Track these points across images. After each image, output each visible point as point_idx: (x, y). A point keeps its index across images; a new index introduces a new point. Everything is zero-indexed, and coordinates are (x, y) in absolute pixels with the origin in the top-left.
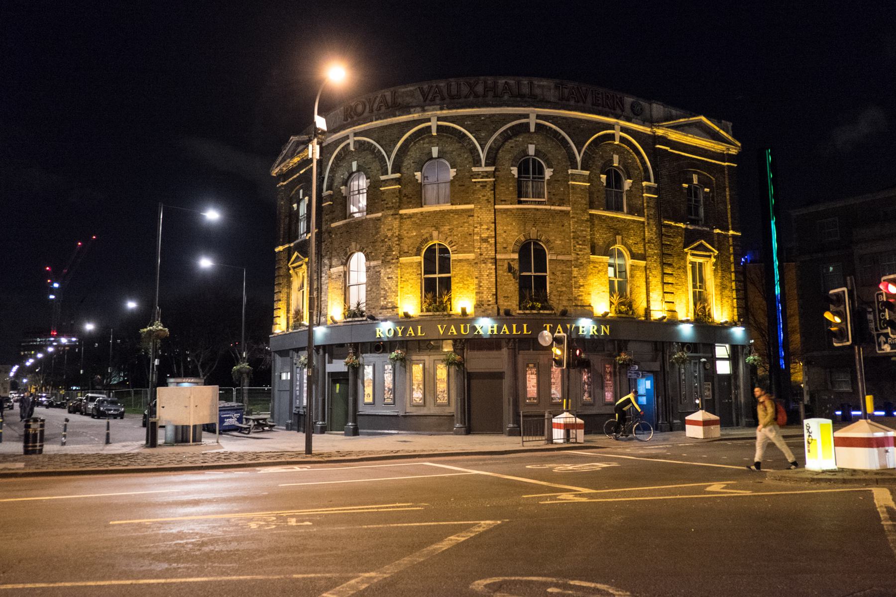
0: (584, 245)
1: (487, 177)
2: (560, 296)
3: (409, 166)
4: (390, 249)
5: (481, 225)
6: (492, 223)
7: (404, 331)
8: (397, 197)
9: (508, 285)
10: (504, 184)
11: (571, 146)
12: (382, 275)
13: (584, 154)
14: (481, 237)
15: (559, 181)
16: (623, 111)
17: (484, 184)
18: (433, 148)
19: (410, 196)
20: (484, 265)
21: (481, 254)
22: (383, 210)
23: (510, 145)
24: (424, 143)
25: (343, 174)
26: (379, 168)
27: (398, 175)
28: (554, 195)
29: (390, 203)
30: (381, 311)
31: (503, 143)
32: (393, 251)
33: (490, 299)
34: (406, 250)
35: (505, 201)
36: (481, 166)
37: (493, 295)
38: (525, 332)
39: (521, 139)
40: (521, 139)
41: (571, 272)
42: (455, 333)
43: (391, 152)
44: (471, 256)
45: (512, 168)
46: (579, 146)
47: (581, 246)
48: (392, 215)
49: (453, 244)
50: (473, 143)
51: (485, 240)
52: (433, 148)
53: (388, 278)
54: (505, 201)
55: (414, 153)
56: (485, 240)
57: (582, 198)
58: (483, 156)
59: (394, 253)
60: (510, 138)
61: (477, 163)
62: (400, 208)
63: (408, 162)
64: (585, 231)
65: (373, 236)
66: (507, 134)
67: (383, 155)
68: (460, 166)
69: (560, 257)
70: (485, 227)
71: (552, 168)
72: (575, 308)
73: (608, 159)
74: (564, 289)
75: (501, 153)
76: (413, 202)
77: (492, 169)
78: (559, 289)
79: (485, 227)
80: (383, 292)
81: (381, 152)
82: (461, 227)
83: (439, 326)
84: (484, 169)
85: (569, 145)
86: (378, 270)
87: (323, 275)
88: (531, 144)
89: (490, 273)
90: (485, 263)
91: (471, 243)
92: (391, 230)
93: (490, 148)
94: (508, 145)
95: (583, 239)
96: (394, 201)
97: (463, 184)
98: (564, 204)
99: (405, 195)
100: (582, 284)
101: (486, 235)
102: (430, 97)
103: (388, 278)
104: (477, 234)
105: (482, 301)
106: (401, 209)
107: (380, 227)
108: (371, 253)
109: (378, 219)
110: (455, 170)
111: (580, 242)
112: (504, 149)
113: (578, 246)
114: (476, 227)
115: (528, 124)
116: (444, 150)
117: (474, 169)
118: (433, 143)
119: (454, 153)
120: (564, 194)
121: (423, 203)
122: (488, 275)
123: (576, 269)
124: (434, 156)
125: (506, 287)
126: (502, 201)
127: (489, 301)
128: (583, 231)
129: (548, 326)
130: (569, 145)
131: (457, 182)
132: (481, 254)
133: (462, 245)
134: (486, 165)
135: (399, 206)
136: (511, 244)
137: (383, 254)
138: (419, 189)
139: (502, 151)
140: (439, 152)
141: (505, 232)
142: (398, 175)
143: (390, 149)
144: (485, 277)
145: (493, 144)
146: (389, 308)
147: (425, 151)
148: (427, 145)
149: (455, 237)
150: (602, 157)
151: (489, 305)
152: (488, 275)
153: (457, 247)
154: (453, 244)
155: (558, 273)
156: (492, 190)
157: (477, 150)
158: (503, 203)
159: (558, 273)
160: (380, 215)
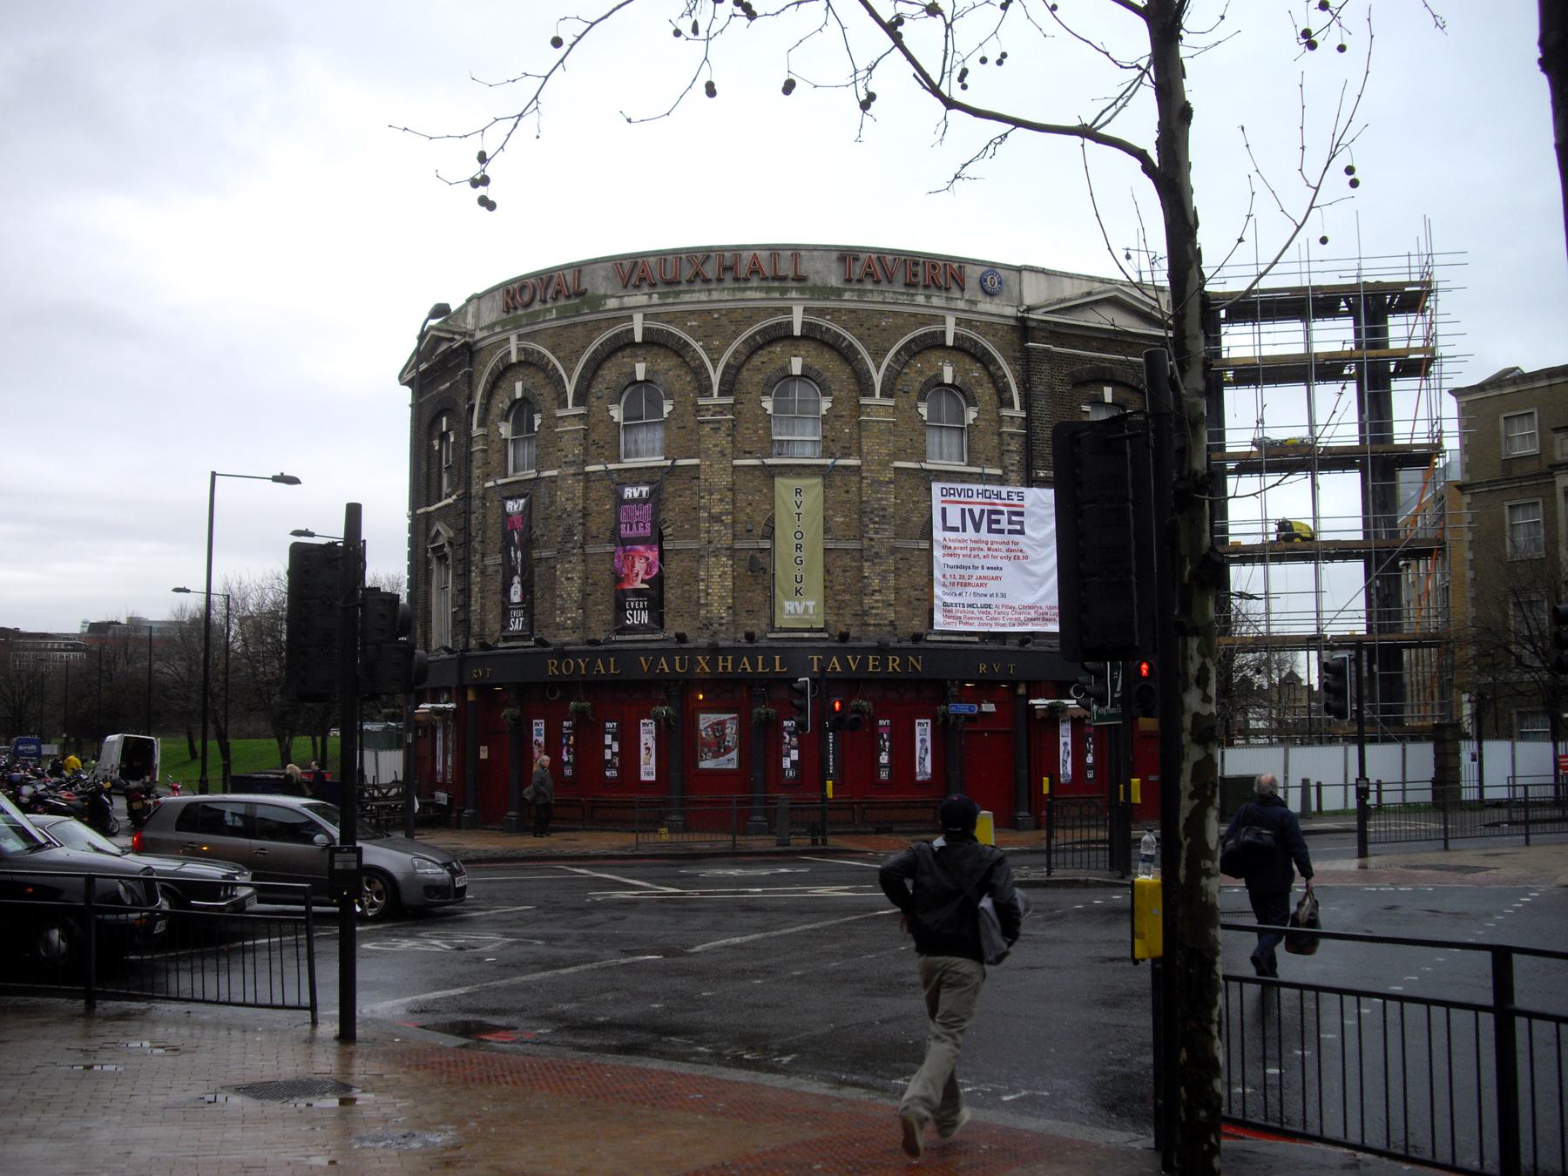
0: (883, 524)
1: (721, 413)
2: (839, 608)
3: (600, 394)
4: (569, 532)
5: (711, 494)
6: (729, 490)
7: (589, 666)
8: (581, 445)
9: (753, 591)
10: (750, 425)
11: (862, 358)
12: (558, 573)
13: (886, 370)
14: (709, 513)
15: (842, 416)
16: (963, 290)
17: (717, 426)
18: (637, 365)
19: (602, 443)
20: (714, 559)
21: (710, 542)
22: (560, 467)
23: (761, 359)
24: (623, 357)
25: (502, 402)
26: (553, 395)
27: (581, 410)
28: (833, 440)
29: (571, 456)
30: (556, 632)
31: (749, 357)
32: (574, 535)
33: (724, 615)
34: (595, 533)
35: (750, 453)
36: (712, 395)
37: (729, 608)
38: (778, 669)
39: (778, 349)
40: (778, 349)
41: (860, 569)
42: (667, 670)
43: (572, 369)
44: (694, 546)
45: (763, 398)
46: (878, 355)
47: (877, 526)
48: (574, 475)
49: (666, 525)
50: (700, 358)
51: (715, 519)
52: (637, 365)
53: (568, 579)
54: (750, 453)
55: (610, 373)
56: (715, 519)
57: (880, 445)
58: (716, 379)
59: (576, 538)
60: (761, 347)
61: (705, 390)
62: (585, 463)
63: (599, 387)
64: (886, 499)
65: (547, 509)
66: (755, 340)
67: (561, 376)
68: (680, 396)
69: (841, 545)
70: (716, 496)
71: (830, 395)
72: (864, 628)
73: (932, 374)
74: (847, 597)
75: (745, 374)
76: (607, 453)
77: (730, 400)
78: (839, 598)
79: (716, 496)
80: (559, 602)
81: (557, 370)
82: (680, 496)
83: (642, 659)
84: (716, 399)
85: (859, 357)
86: (552, 565)
87: (473, 568)
88: (795, 356)
89: (724, 573)
90: (716, 556)
91: (695, 522)
92: (572, 499)
93: (727, 366)
94: (757, 360)
95: (881, 513)
96: (576, 452)
97: (682, 425)
98: (850, 455)
99: (594, 443)
100: (877, 588)
101: (718, 511)
102: (633, 281)
103: (568, 579)
104: (704, 508)
105: (711, 618)
106: (588, 465)
107: (556, 495)
108: (543, 535)
109: (553, 479)
110: (672, 402)
111: (877, 519)
112: (751, 367)
113: (872, 526)
114: (703, 497)
115: (790, 324)
116: (656, 368)
117: (701, 402)
118: (637, 356)
119: (671, 373)
120: (851, 437)
121: (622, 455)
122: (720, 576)
123: (868, 564)
124: (638, 379)
125: (749, 594)
126: (745, 452)
127: (723, 618)
128: (882, 499)
129: (815, 657)
130: (859, 357)
131: (674, 422)
132: (710, 542)
133: (682, 526)
134: (721, 394)
135: (584, 461)
136: (759, 523)
137: (559, 539)
138: (615, 433)
139: (748, 370)
140: (647, 371)
141: (750, 504)
142: (581, 410)
143: (572, 366)
144: (716, 579)
145: (732, 359)
146: (567, 629)
147: (624, 370)
148: (629, 360)
149: (671, 513)
150: (921, 372)
151: (721, 625)
152: (720, 576)
153: (673, 530)
154: (666, 525)
155: (838, 571)
156: (728, 435)
157: (707, 369)
158: (748, 455)
159: (838, 571)
160: (554, 473)
